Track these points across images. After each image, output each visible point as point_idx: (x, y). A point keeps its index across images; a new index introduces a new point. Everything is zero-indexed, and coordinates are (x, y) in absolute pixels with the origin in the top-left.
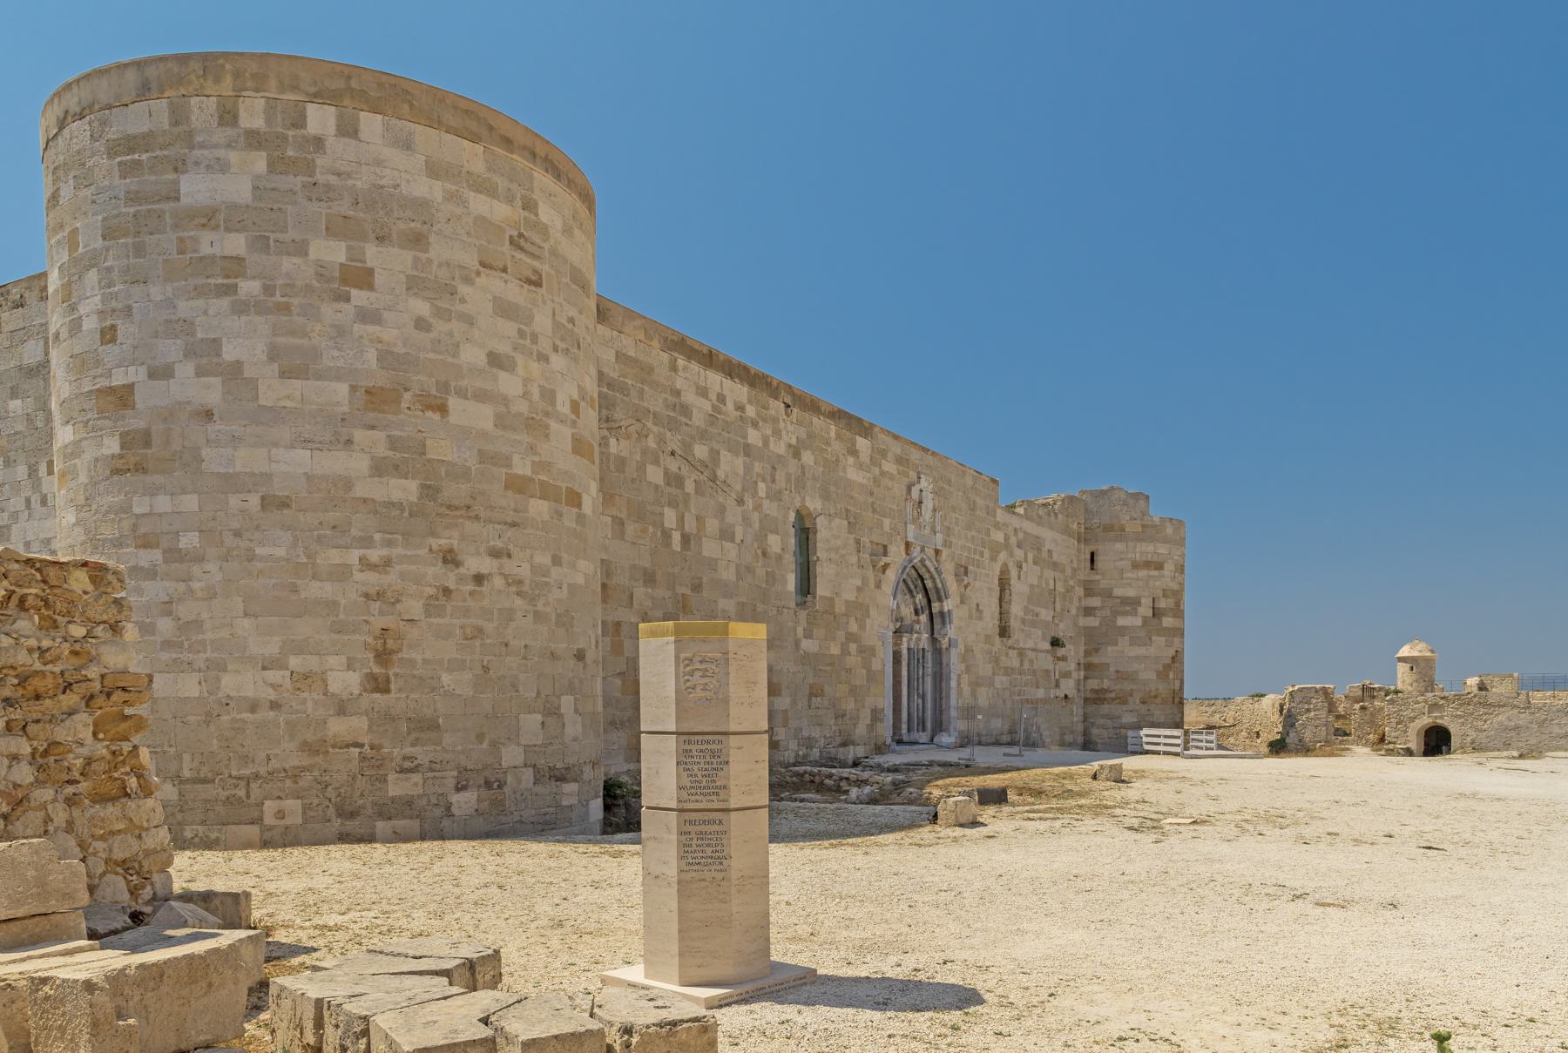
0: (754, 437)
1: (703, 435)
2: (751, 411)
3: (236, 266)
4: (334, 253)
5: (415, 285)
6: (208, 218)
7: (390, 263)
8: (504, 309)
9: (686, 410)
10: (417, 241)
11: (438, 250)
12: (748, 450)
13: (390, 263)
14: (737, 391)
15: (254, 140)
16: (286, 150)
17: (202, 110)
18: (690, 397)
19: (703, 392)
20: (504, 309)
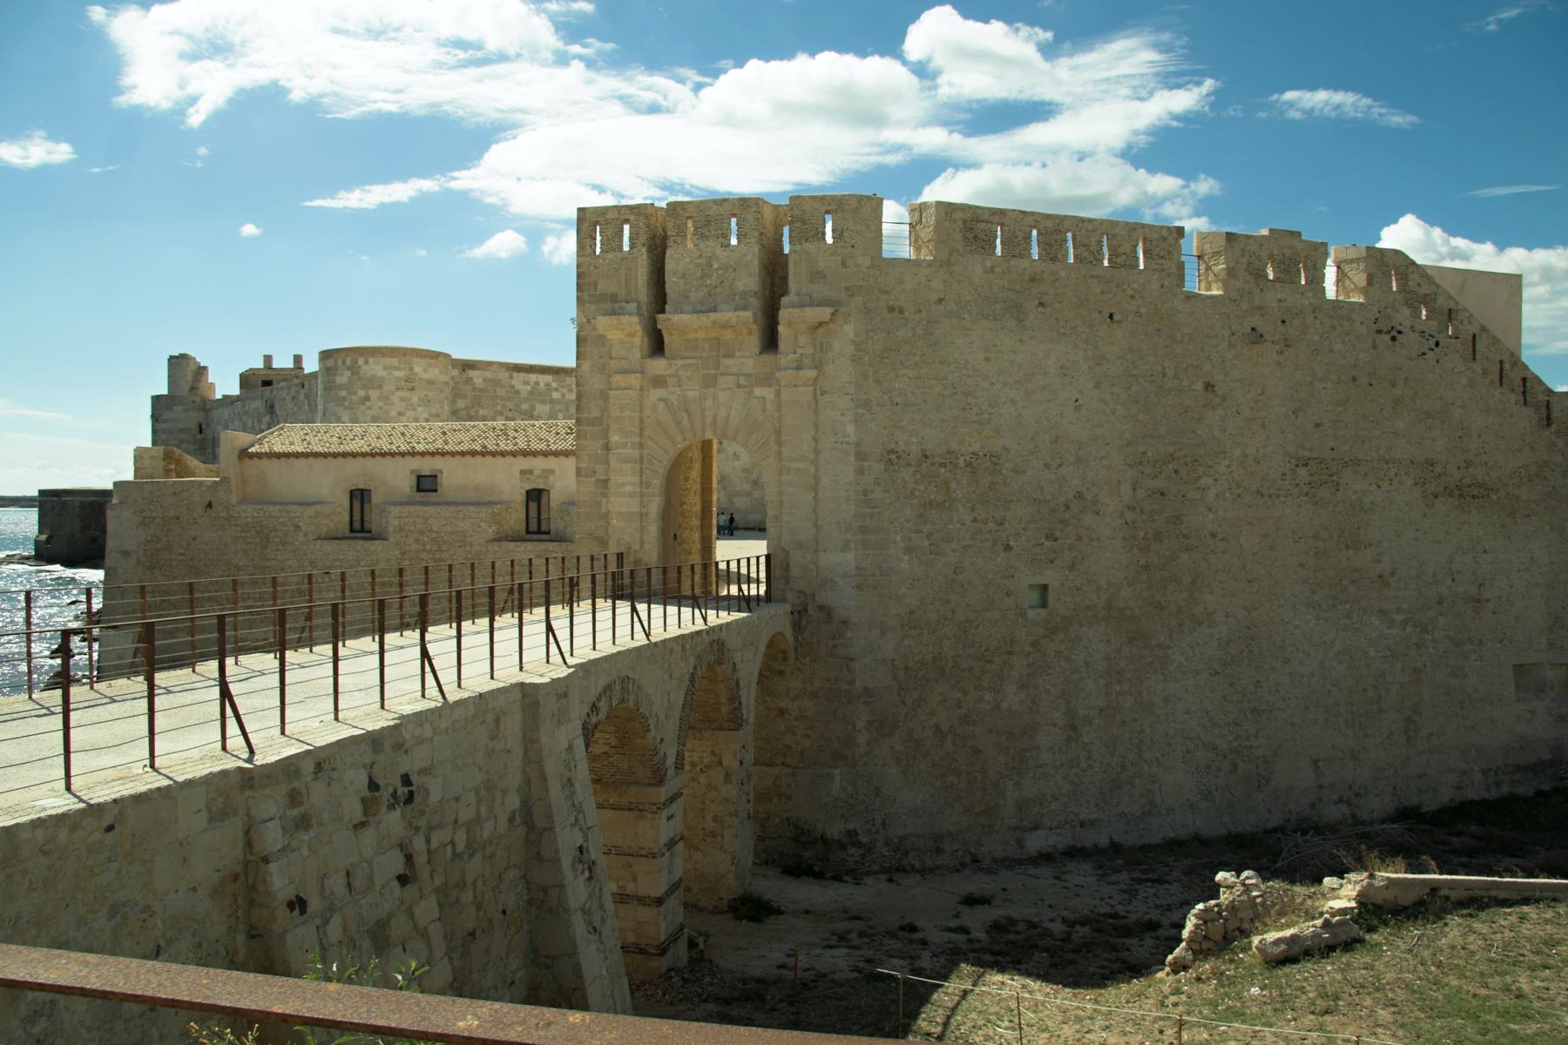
0: (556, 395)
1: (526, 400)
2: (554, 385)
3: (344, 398)
4: (362, 393)
5: (379, 398)
6: (340, 387)
7: (374, 394)
8: (402, 399)
9: (518, 392)
10: (380, 387)
11: (386, 388)
12: (552, 401)
13: (374, 394)
14: (549, 378)
15: (349, 368)
16: (354, 370)
17: (340, 362)
18: (519, 386)
19: (527, 383)
20: (402, 399)
